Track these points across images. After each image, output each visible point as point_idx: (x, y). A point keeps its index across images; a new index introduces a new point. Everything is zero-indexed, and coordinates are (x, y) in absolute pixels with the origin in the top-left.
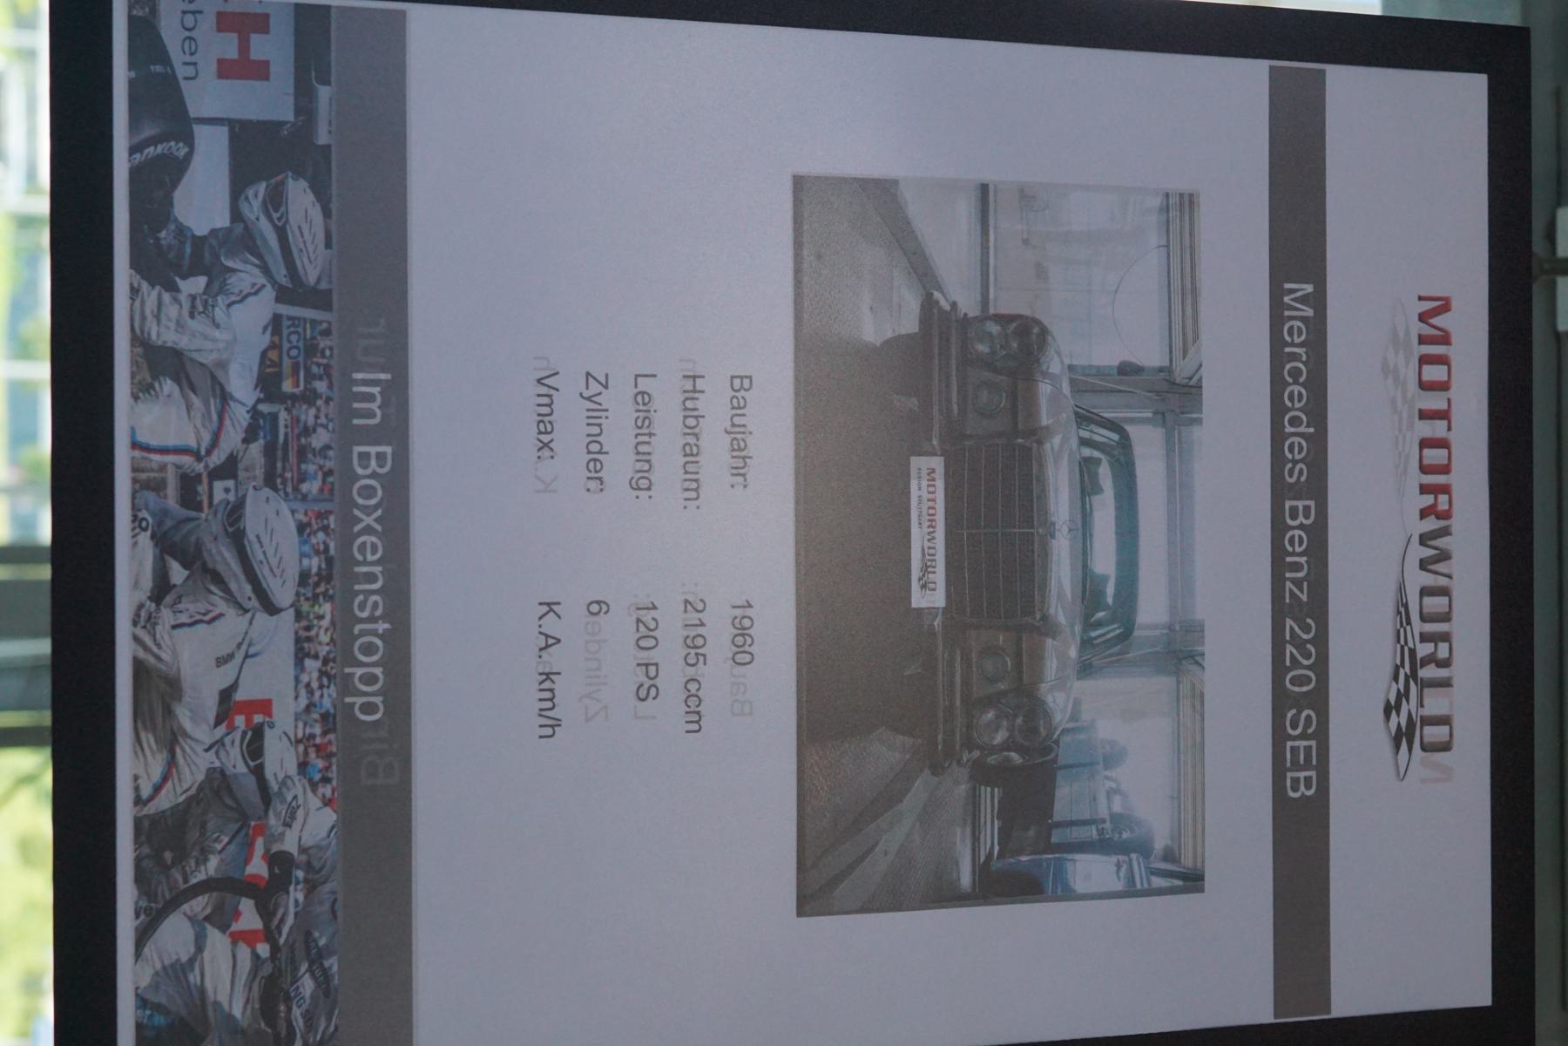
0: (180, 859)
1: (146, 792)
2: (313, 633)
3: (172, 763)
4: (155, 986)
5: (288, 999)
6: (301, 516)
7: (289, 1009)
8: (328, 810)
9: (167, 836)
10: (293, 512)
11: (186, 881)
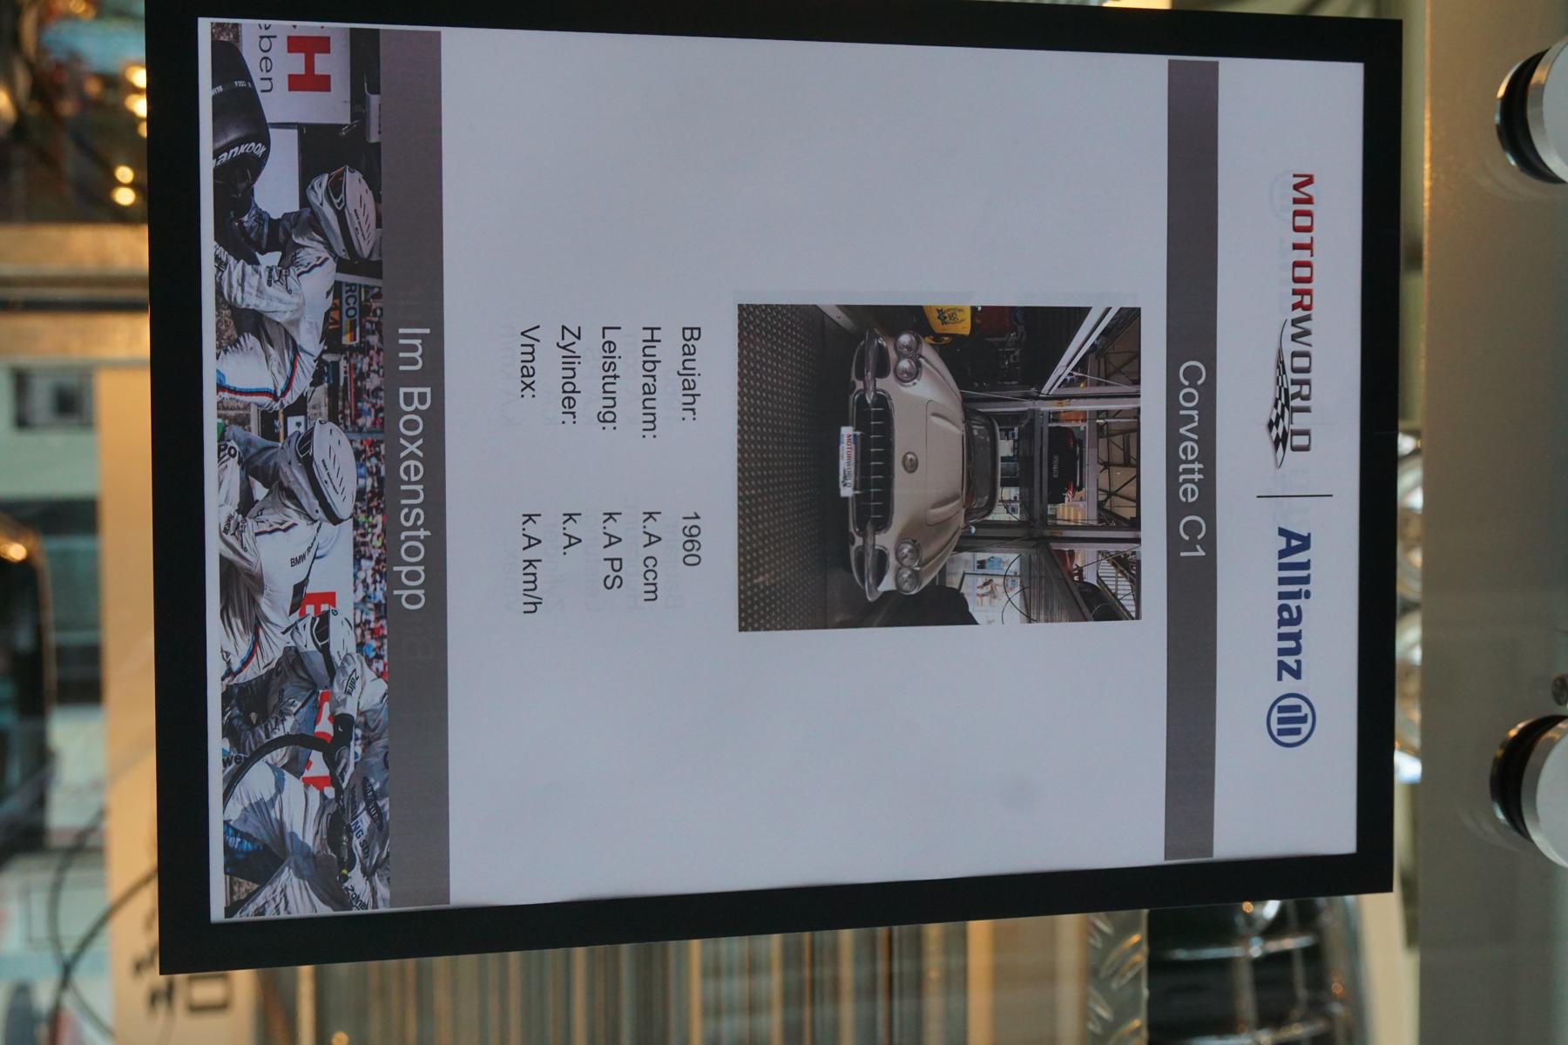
0: (264, 718)
1: (236, 666)
2: (368, 539)
3: (256, 642)
4: (244, 819)
5: (349, 831)
6: (358, 445)
7: (350, 839)
8: (381, 681)
9: (252, 701)
10: (351, 442)
11: (268, 736)
